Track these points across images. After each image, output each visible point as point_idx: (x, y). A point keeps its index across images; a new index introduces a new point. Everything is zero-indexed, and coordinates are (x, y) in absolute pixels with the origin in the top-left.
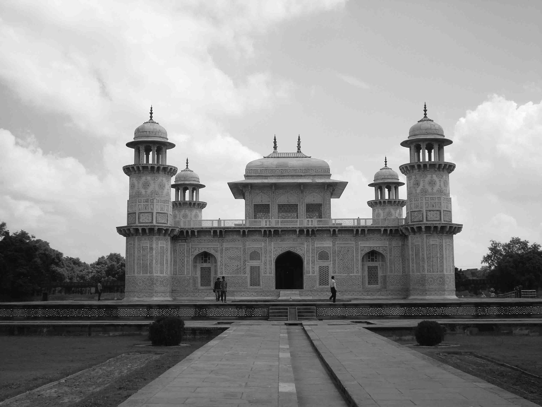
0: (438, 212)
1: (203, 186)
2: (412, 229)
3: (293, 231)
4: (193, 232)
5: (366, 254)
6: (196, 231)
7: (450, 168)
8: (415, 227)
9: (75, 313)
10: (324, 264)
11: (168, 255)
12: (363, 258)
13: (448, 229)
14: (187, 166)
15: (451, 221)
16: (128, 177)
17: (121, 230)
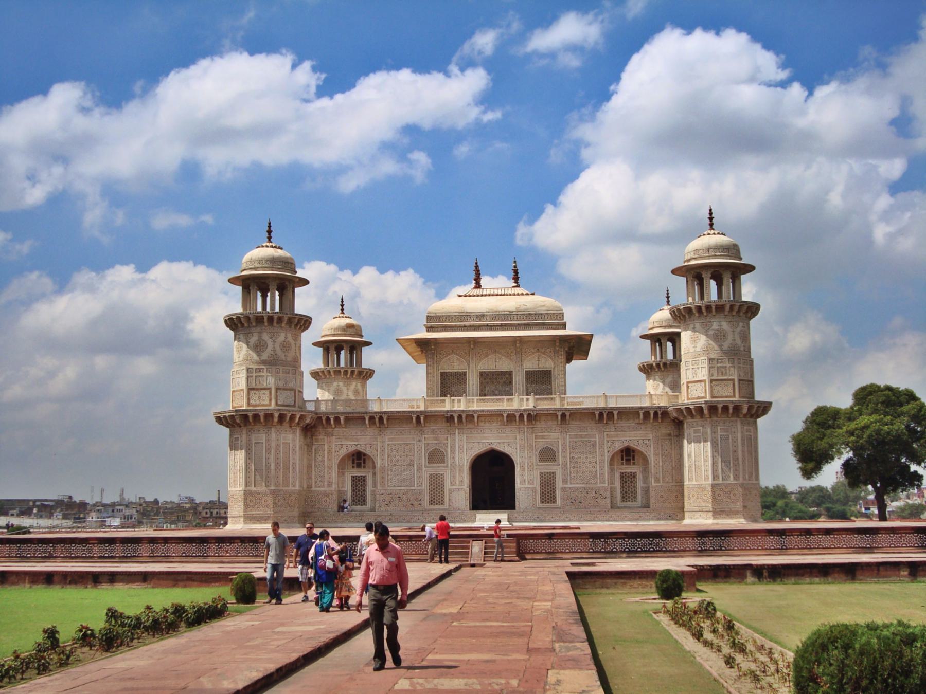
0: (730, 383)
1: (368, 344)
2: (688, 409)
3: (496, 416)
4: (337, 419)
5: (617, 453)
6: (342, 418)
7: (752, 309)
8: (692, 407)
9: (118, 550)
10: (549, 467)
11: (297, 458)
12: (612, 459)
13: (745, 411)
14: (342, 310)
15: (753, 397)
16: (232, 333)
17: (220, 420)
